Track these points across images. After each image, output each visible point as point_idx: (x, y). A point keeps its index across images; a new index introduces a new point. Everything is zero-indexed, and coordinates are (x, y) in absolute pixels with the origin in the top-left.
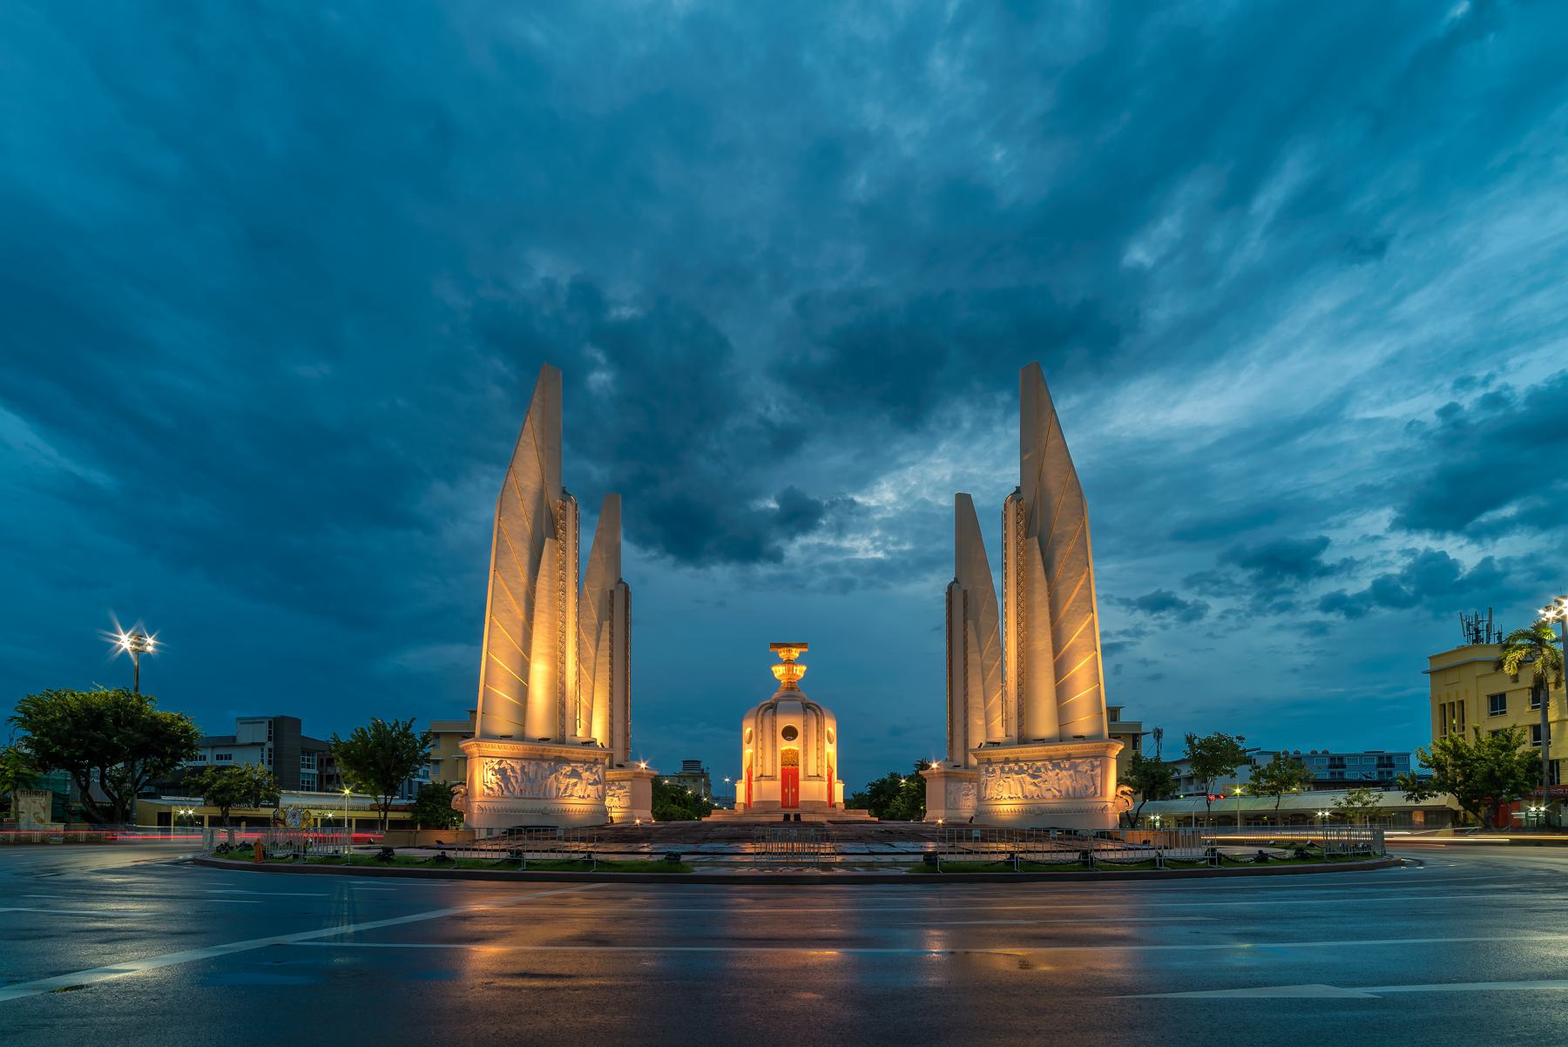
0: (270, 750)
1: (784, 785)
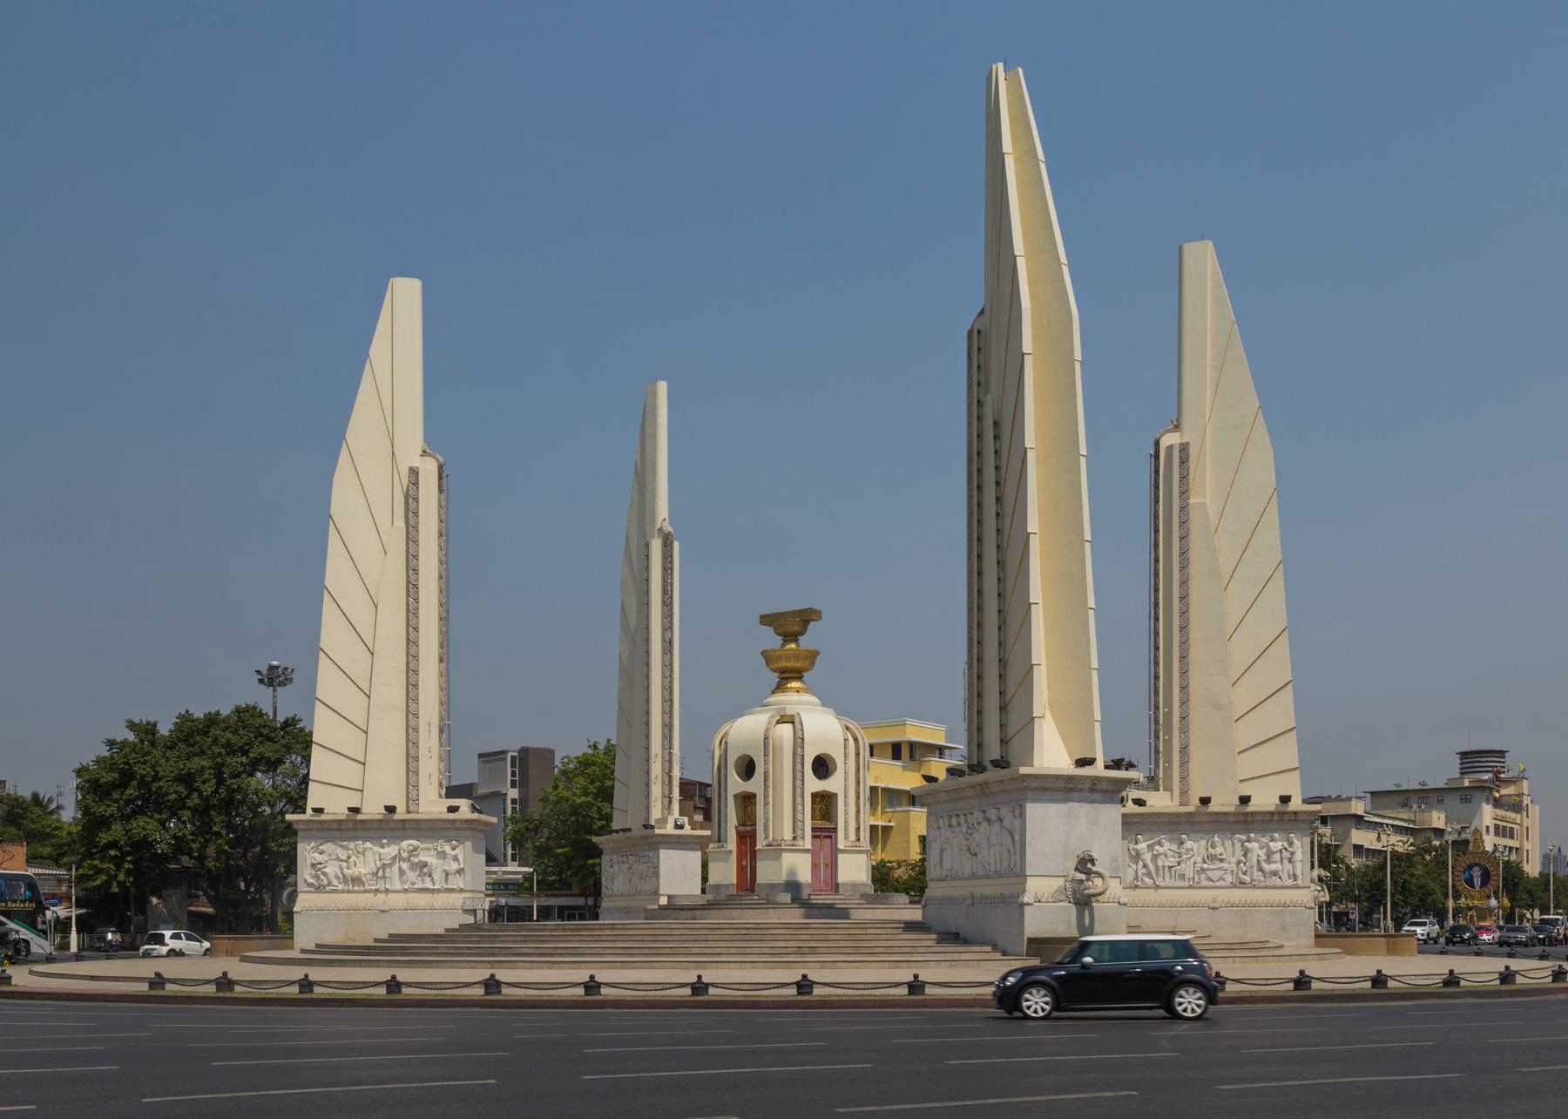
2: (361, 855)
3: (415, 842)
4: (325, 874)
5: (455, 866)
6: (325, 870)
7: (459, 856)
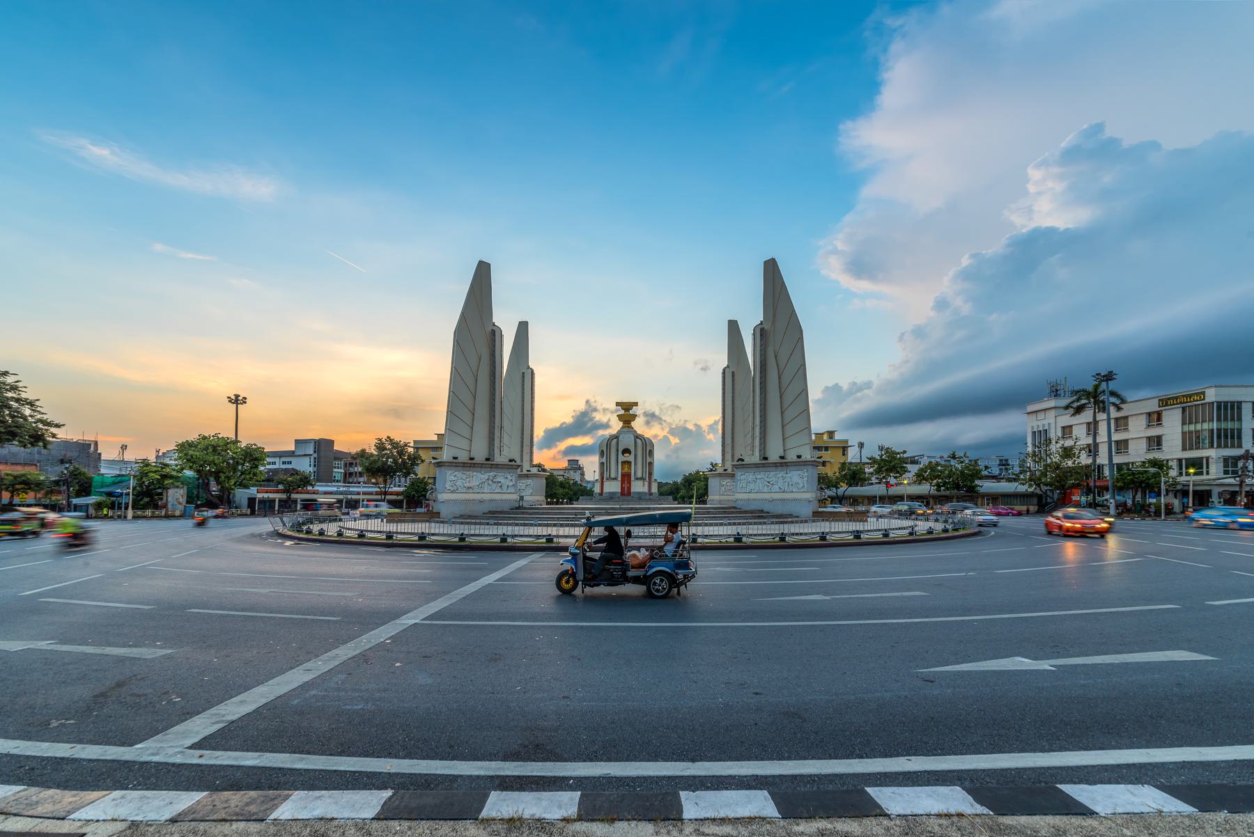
0: (315, 458)
1: (623, 482)
5: (511, 484)
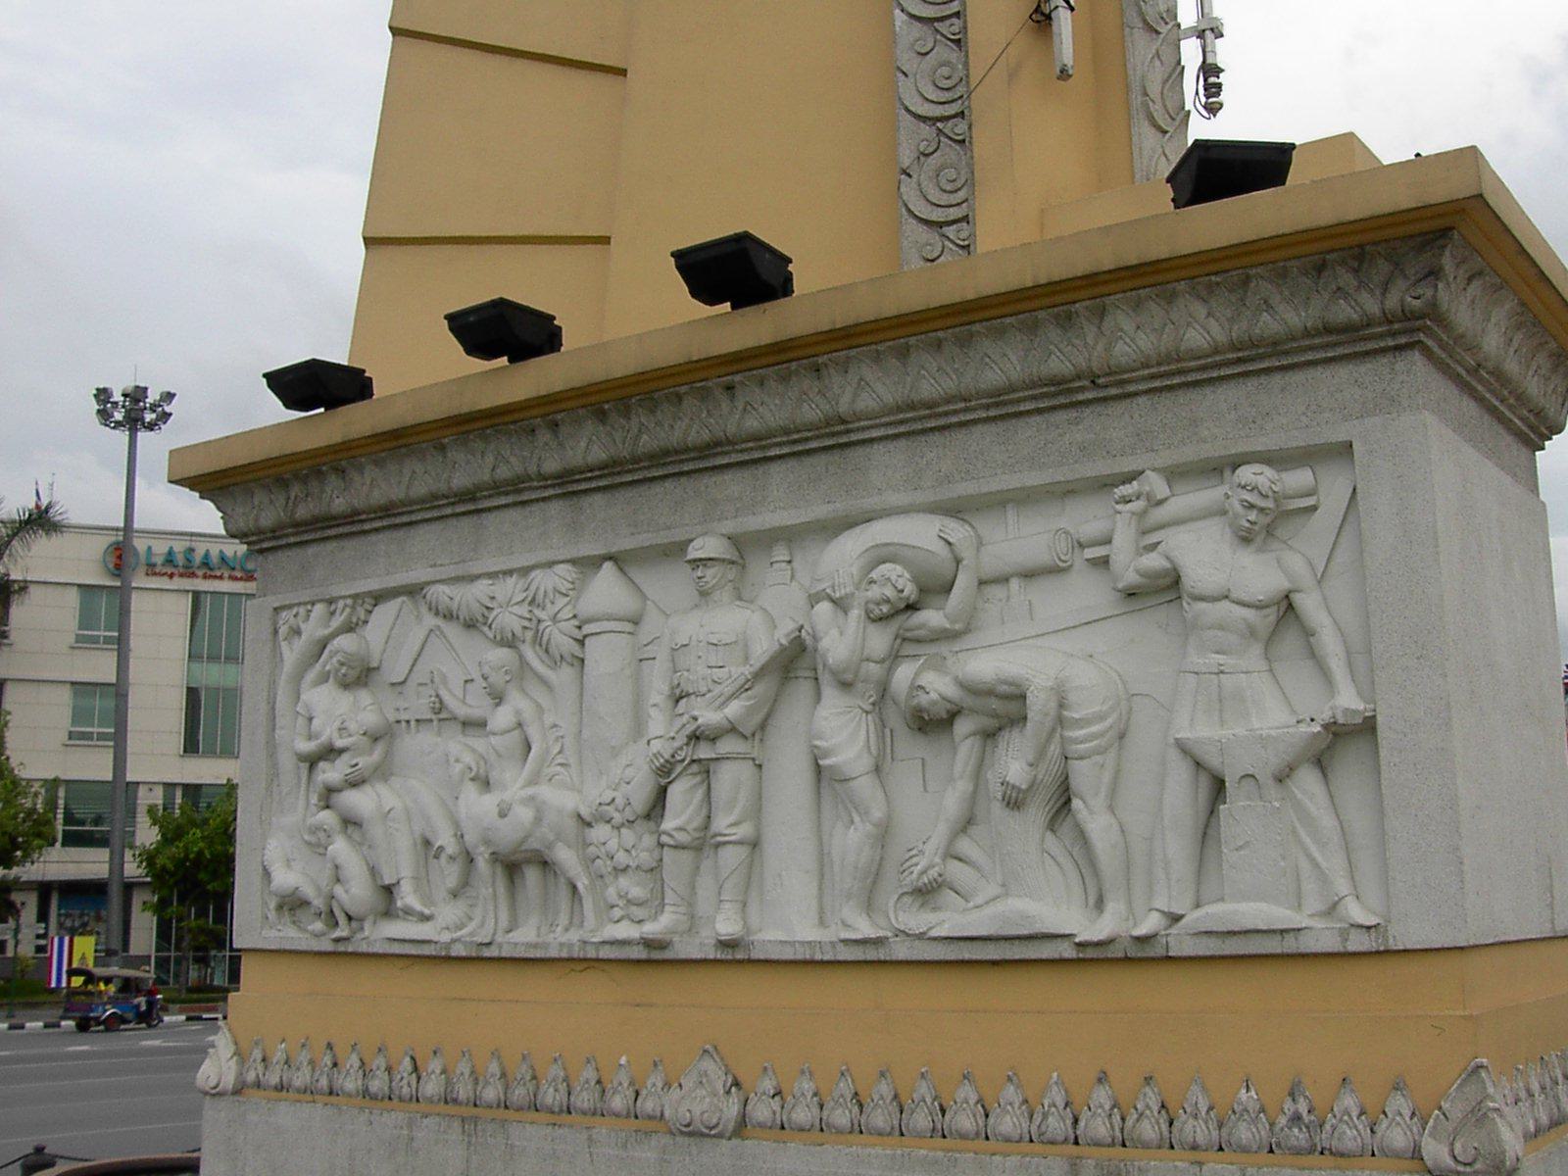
2: (564, 676)
3: (922, 533)
4: (350, 822)
6: (359, 801)
7: (1309, 604)
